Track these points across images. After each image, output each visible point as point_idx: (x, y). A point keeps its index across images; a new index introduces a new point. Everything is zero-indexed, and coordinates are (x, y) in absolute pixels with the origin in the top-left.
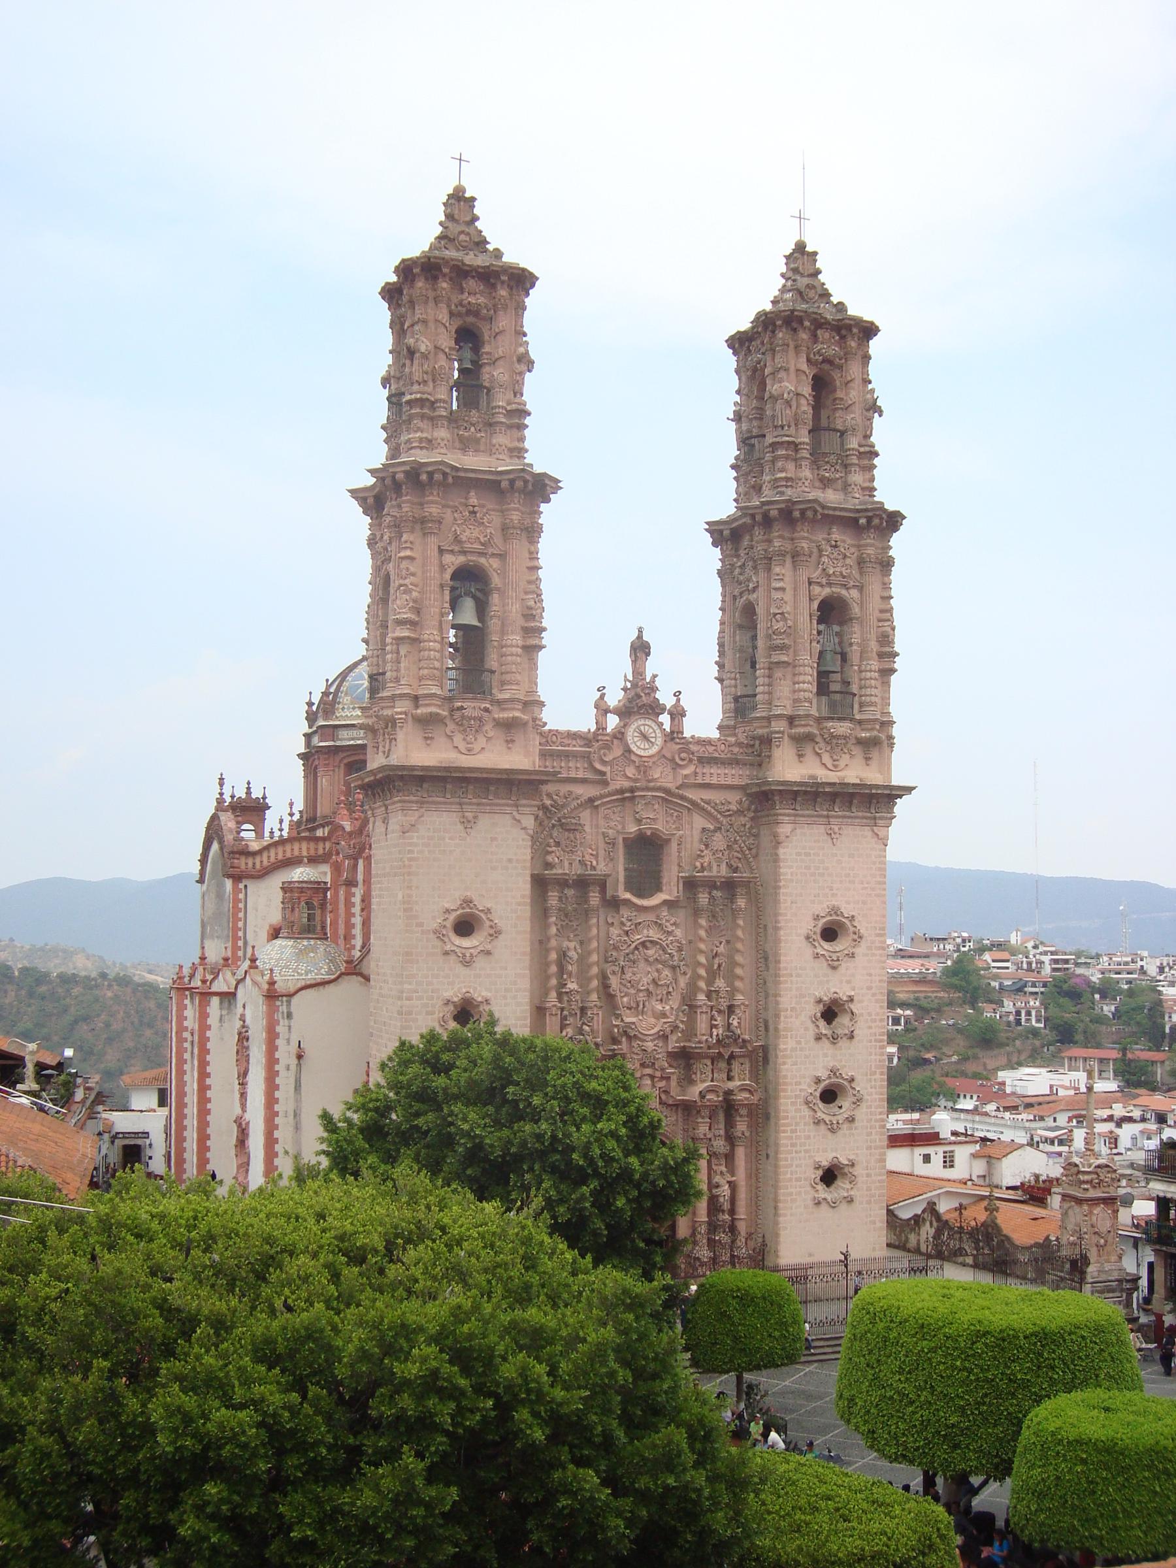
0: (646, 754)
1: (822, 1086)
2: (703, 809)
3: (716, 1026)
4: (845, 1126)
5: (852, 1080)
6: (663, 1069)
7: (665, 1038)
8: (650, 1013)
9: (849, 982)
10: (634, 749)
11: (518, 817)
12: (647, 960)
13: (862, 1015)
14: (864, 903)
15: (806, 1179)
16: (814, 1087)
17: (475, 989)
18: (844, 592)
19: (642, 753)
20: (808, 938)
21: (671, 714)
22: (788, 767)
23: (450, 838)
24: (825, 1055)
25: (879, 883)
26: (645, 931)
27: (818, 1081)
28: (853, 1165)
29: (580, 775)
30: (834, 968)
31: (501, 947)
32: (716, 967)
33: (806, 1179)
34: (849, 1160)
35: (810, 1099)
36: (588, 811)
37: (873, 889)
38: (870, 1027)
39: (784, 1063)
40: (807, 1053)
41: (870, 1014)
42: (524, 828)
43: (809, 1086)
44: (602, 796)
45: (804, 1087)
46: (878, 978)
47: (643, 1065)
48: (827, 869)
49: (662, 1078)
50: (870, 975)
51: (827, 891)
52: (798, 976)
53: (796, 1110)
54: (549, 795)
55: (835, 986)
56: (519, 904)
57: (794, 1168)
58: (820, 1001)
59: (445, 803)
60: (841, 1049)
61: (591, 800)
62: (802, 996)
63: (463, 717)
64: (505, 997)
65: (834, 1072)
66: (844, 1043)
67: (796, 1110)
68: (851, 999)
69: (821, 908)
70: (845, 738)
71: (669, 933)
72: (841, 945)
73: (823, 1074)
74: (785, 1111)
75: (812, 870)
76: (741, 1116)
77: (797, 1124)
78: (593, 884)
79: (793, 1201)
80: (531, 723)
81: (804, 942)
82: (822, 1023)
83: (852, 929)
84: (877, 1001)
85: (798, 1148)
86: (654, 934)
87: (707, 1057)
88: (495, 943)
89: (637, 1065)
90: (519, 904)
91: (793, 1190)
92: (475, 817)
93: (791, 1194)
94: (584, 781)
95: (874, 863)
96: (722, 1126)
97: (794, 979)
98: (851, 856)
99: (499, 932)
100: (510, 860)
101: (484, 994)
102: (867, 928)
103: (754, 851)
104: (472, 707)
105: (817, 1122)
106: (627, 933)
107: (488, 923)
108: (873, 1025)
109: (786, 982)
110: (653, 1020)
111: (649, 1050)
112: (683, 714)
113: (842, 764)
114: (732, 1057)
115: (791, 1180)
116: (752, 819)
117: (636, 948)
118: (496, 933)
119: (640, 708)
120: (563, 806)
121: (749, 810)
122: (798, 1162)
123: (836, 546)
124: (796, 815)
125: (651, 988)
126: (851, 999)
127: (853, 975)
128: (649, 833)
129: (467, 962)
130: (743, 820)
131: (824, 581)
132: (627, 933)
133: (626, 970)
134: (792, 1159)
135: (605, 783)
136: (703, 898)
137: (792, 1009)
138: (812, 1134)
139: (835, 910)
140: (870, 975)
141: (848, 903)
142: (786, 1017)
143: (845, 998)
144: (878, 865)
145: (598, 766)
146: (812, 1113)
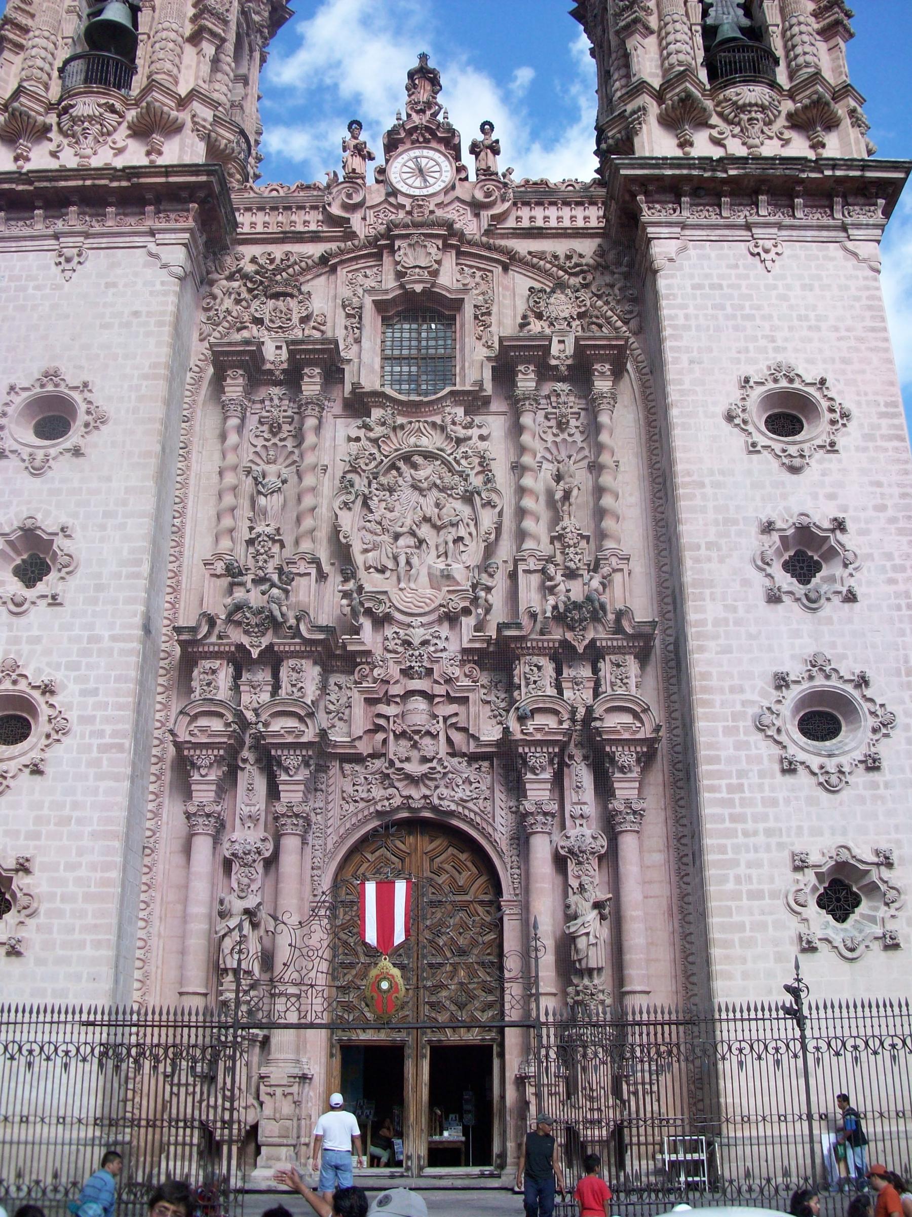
0: (425, 192)
1: (793, 694)
2: (533, 266)
3: (552, 590)
4: (860, 778)
5: (863, 682)
6: (449, 681)
7: (452, 618)
8: (424, 579)
9: (832, 497)
10: (404, 189)
11: (152, 247)
12: (414, 487)
13: (870, 557)
14: (844, 361)
15: (774, 895)
16: (775, 694)
17: (47, 513)
19: (417, 192)
20: (730, 418)
21: (475, 149)
22: (656, 142)
23: (37, 288)
24: (796, 634)
25: (873, 329)
26: (413, 440)
27: (782, 682)
28: (890, 865)
29: (313, 227)
30: (795, 470)
31: (98, 444)
32: (559, 495)
33: (774, 895)
34: (877, 853)
35: (767, 720)
36: (323, 279)
37: (860, 340)
38: (892, 581)
39: (701, 649)
40: (753, 629)
41: (889, 556)
42: (164, 266)
43: (764, 694)
44: (342, 252)
45: (748, 696)
46: (896, 491)
47: (407, 673)
48: (759, 308)
49: (451, 699)
50: (879, 484)
51: (762, 343)
53: (738, 746)
54: (254, 260)
56: (146, 377)
57: (742, 870)
58: (768, 528)
59: (32, 238)
60: (829, 621)
61: (324, 260)
63: (75, 120)
64: (103, 527)
65: (817, 665)
66: (832, 609)
67: (738, 746)
68: (840, 525)
69: (757, 370)
70: (763, 108)
71: (459, 441)
73: (796, 670)
74: (711, 746)
75: (729, 310)
76: (622, 769)
77: (741, 774)
78: (312, 363)
79: (747, 943)
80: (189, 125)
81: (726, 427)
82: (786, 581)
83: (825, 404)
85: (750, 826)
86: (431, 441)
87: (541, 651)
88: (94, 437)
89: (394, 671)
90: (146, 377)
91: (747, 919)
92: (79, 255)
93: (741, 927)
94: (315, 237)
95: (857, 299)
96: (588, 793)
97: (709, 490)
99: (102, 420)
100: (136, 314)
101: (64, 520)
102: (859, 403)
103: (633, 324)
104: (85, 106)
105: (789, 768)
106: (375, 441)
107: (82, 407)
108: (900, 576)
109: (692, 497)
110: (429, 591)
111: (416, 642)
112: (495, 149)
114: (594, 655)
115: (736, 896)
116: (627, 276)
117: (393, 466)
118: (98, 420)
119: (410, 132)
120: (278, 271)
121: (619, 264)
122: (752, 856)
125: (425, 531)
126: (840, 525)
128: (418, 288)
129: (37, 471)
130: (608, 279)
132: (375, 441)
133: (373, 504)
134: (737, 848)
135: (352, 235)
136: (526, 381)
137: (710, 546)
138: (780, 796)
140: (879, 484)
141: (811, 361)
142: (697, 560)
143: (826, 525)
144: (864, 302)
145: (336, 210)
146: (776, 751)
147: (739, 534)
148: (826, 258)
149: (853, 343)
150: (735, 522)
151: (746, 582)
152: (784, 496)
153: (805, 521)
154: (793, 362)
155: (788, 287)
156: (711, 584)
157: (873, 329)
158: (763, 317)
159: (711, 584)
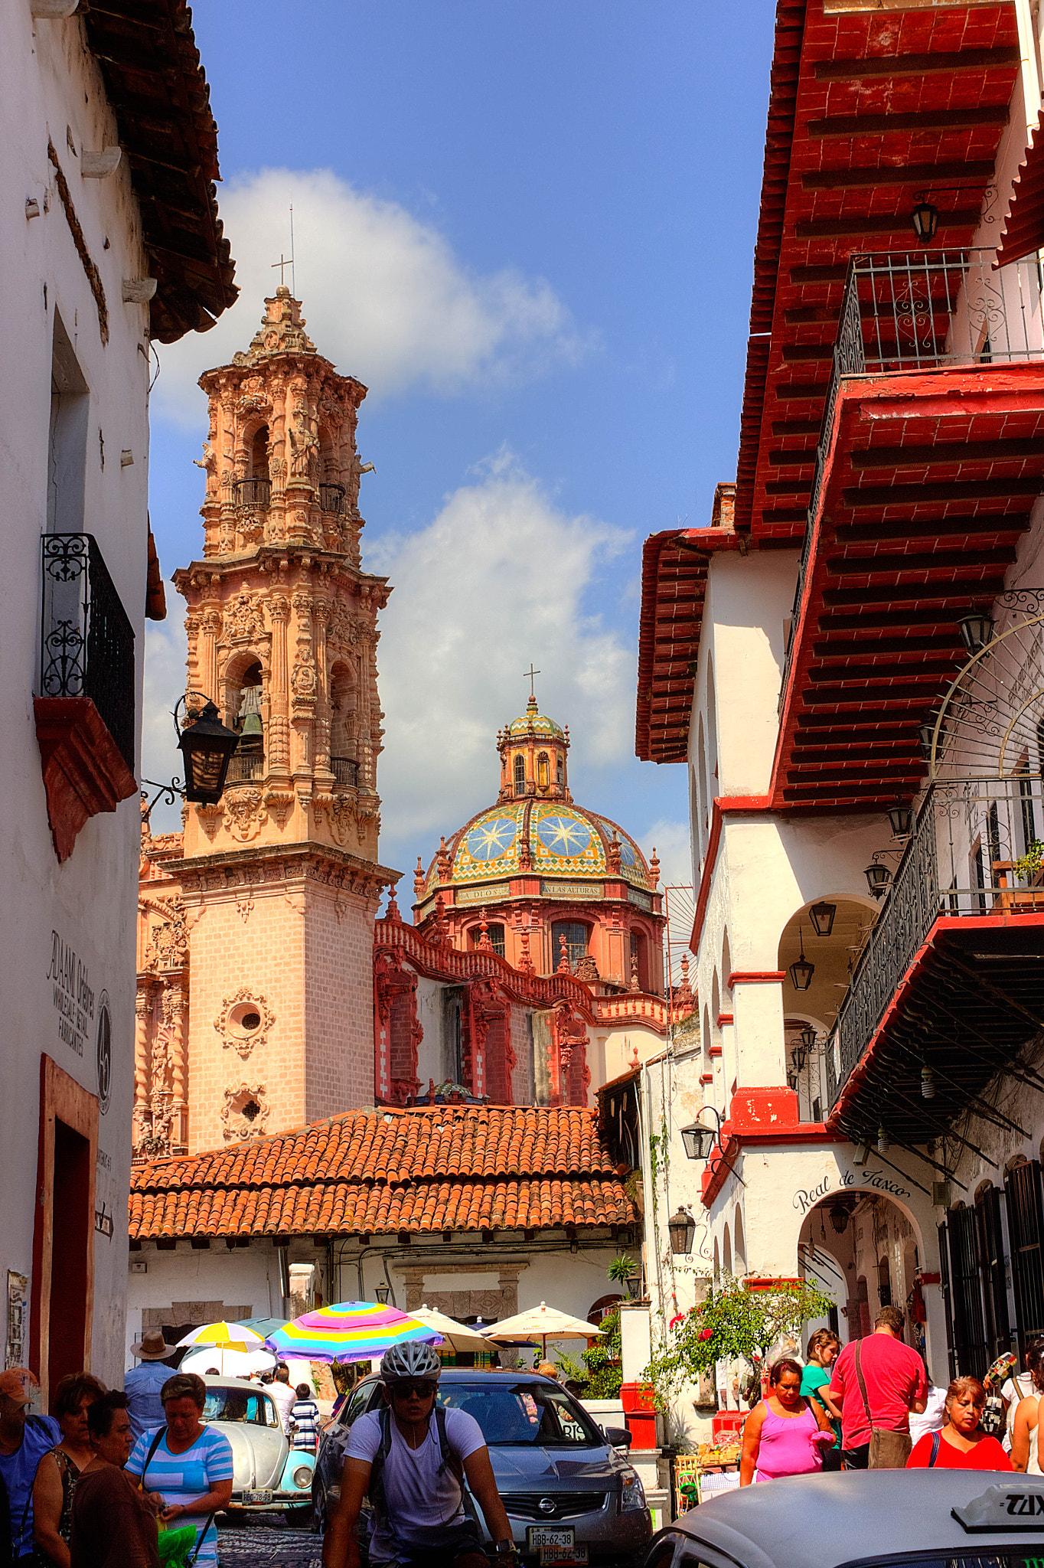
9: (260, 1071)
14: (277, 980)
18: (252, 649)
30: (245, 1057)
37: (287, 964)
41: (284, 1105)
46: (292, 1063)
50: (284, 1060)
51: (237, 972)
52: (207, 1069)
55: (247, 1077)
62: (212, 1090)
68: (261, 1091)
69: (230, 993)
72: (258, 1032)
84: (292, 1090)
95: (288, 935)
97: (203, 1073)
98: (264, 931)
113: (251, 833)
123: (243, 603)
124: (203, 897)
127: (264, 1063)
131: (228, 644)
137: (201, 1106)
139: (245, 993)
140: (284, 1060)
141: (259, 983)
147: (215, 1098)
148: (277, 907)
149: (282, 967)
150: (212, 1090)
151: (216, 1127)
152: (238, 1072)
153: (243, 1088)
154: (250, 985)
155: (254, 932)
156: (200, 1128)
157: (294, 956)
158: (242, 955)
159: (200, 1128)
